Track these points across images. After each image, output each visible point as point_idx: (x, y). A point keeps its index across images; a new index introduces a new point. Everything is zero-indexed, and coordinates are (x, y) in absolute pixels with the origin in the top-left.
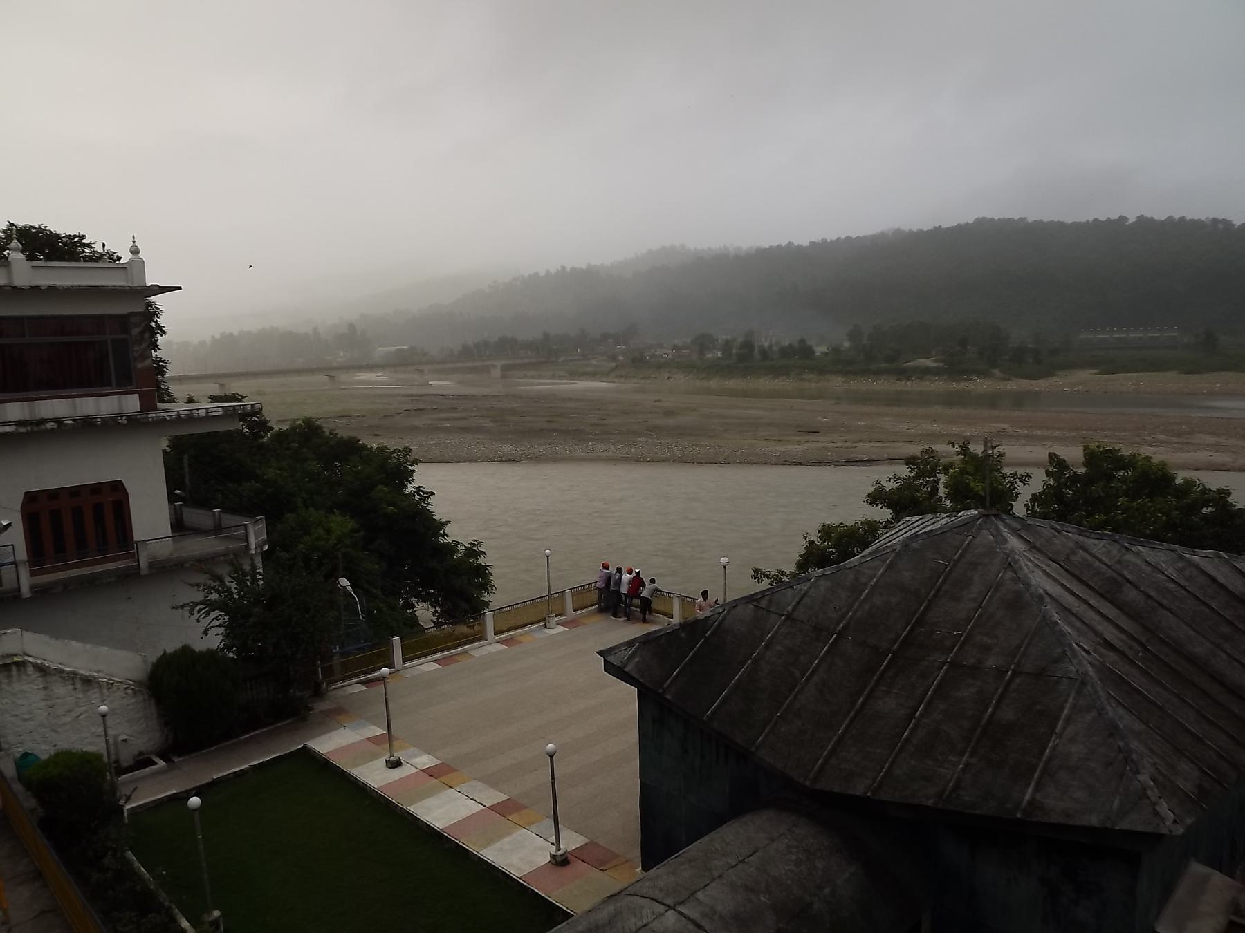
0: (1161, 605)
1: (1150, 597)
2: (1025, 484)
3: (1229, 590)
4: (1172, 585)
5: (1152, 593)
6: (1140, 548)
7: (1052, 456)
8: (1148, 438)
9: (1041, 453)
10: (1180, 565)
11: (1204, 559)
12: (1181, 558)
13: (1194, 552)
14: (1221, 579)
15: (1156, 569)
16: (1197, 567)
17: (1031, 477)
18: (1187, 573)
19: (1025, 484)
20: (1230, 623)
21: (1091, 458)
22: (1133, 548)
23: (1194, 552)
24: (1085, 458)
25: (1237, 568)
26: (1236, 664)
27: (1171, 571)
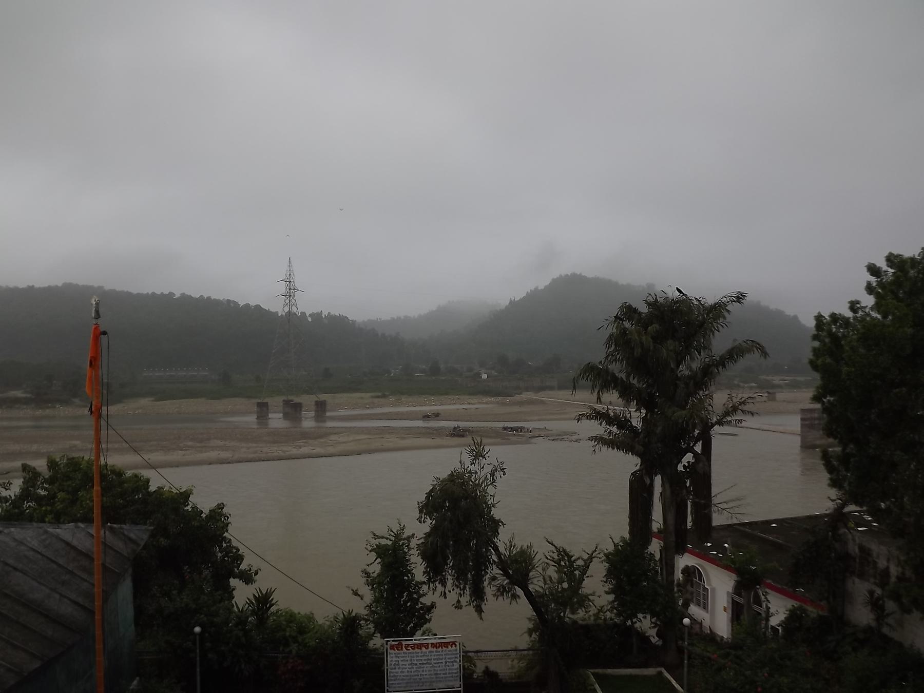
0: (15, 569)
1: (7, 564)
2: (6, 490)
3: (77, 549)
4: (31, 553)
5: (11, 561)
6: (12, 529)
7: (25, 468)
8: (181, 445)
9: (18, 464)
10: (43, 537)
11: (66, 531)
12: (46, 532)
13: (58, 526)
14: (75, 543)
15: (21, 543)
16: (58, 537)
17: (11, 483)
18: (47, 542)
19: (6, 490)
20: (71, 572)
21: (52, 464)
22: (6, 531)
23: (58, 526)
24: (48, 466)
25: (90, 533)
26: (65, 600)
27: (35, 544)
